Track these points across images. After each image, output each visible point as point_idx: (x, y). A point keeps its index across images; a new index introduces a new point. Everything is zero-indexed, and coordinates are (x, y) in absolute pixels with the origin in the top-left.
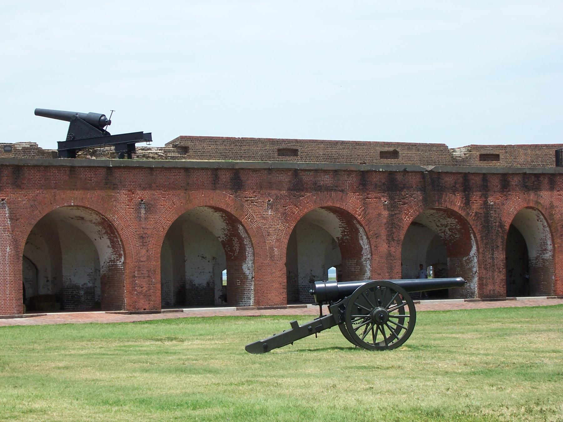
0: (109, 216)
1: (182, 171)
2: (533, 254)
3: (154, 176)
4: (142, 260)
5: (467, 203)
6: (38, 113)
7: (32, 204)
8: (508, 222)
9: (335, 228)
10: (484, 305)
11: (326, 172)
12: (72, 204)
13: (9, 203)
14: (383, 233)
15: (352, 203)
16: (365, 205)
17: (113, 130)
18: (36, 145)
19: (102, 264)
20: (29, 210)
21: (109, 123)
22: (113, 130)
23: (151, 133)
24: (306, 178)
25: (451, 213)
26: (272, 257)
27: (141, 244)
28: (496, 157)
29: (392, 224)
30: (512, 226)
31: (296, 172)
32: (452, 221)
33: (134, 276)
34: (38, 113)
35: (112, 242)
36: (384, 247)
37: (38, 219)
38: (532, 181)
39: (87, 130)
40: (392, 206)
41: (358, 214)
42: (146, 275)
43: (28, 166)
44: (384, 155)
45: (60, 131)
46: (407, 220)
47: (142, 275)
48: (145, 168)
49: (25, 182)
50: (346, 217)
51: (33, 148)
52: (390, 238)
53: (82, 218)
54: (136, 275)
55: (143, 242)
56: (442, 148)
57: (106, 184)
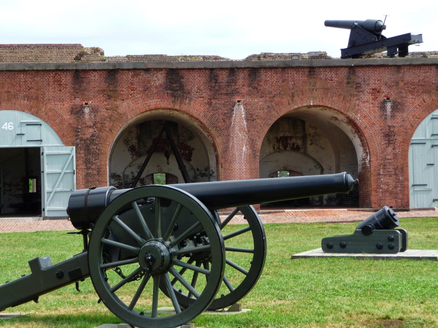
0: (352, 115)
1: (434, 68)
3: (402, 74)
4: (388, 157)
6: (328, 24)
7: (269, 104)
12: (312, 104)
13: (245, 105)
17: (387, 34)
18: (325, 53)
19: (359, 163)
20: (265, 110)
21: (383, 28)
22: (387, 34)
23: (421, 35)
27: (387, 142)
33: (379, 174)
34: (328, 24)
35: (362, 141)
37: (275, 119)
39: (366, 36)
42: (393, 173)
43: (265, 68)
45: (341, 39)
47: (388, 173)
48: (391, 66)
49: (262, 84)
51: (322, 56)
53: (336, 119)
54: (381, 173)
55: (389, 140)
57: (348, 83)
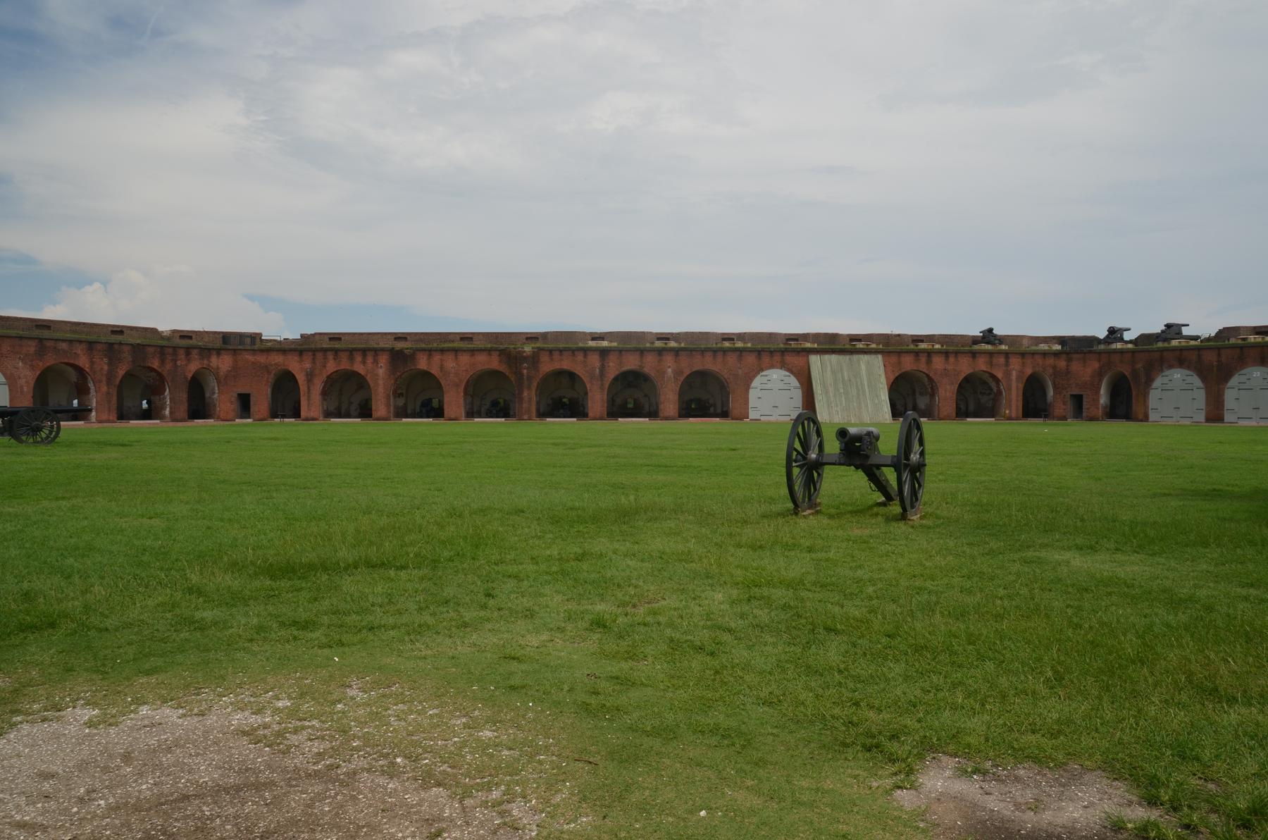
2: (207, 395)
5: (163, 362)
8: (190, 376)
9: (73, 376)
10: (171, 424)
11: (63, 341)
14: (104, 379)
15: (83, 362)
16: (92, 363)
24: (48, 344)
25: (152, 370)
26: (22, 392)
28: (190, 338)
29: (110, 377)
30: (194, 377)
31: (41, 340)
32: (153, 374)
36: (104, 389)
38: (206, 351)
40: (110, 364)
41: (87, 367)
44: (113, 332)
46: (121, 373)
50: (79, 370)
52: (109, 383)
56: (154, 331)
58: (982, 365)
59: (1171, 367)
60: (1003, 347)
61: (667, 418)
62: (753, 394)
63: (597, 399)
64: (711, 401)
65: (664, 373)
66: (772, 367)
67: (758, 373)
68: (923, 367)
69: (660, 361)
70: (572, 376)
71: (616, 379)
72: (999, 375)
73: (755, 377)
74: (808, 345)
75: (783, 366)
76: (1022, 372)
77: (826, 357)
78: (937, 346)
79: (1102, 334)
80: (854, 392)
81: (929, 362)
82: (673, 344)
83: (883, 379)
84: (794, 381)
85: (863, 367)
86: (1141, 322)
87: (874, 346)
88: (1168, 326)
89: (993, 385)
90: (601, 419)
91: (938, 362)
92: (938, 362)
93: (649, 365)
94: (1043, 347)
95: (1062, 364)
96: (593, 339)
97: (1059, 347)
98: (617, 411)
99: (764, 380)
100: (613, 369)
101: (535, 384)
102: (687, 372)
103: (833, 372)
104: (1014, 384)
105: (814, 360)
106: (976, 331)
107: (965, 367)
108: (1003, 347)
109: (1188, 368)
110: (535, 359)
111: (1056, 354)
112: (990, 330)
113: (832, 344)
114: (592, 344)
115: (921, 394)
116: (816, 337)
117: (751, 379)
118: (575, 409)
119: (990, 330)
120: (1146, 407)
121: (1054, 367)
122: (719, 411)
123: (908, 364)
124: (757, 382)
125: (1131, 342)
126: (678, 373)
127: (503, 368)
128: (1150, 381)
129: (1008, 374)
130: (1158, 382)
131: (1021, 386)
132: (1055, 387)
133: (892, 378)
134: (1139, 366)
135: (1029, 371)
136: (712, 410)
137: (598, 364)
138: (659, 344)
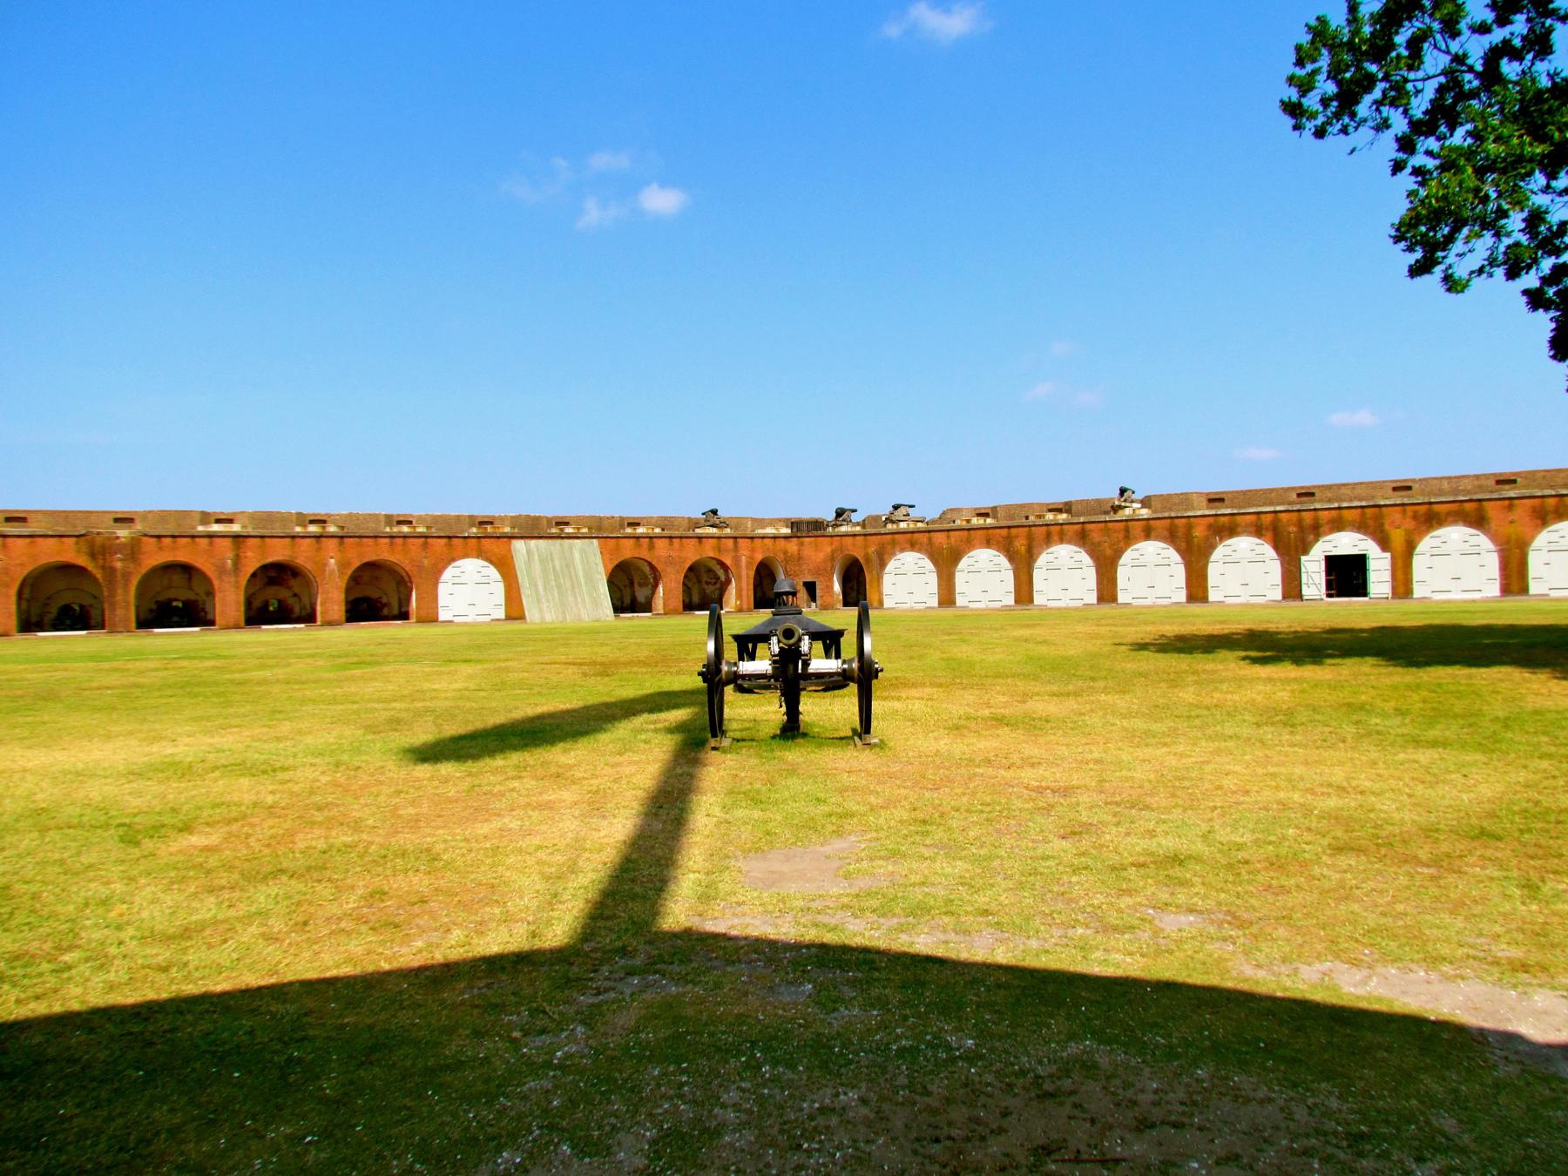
58: (708, 551)
59: (903, 550)
60: (728, 531)
61: (329, 624)
62: (443, 590)
63: (229, 599)
64: (384, 600)
65: (325, 565)
66: (466, 556)
67: (449, 563)
68: (645, 554)
69: (319, 550)
70: (187, 570)
71: (254, 575)
72: (728, 562)
73: (445, 568)
74: (507, 530)
75: (480, 554)
76: (752, 558)
77: (533, 542)
78: (657, 530)
79: (831, 516)
80: (568, 584)
81: (651, 547)
82: (332, 529)
83: (601, 569)
84: (493, 573)
85: (577, 555)
86: (870, 504)
87: (585, 530)
88: (896, 507)
89: (721, 573)
90: (237, 627)
91: (661, 544)
92: (661, 544)
93: (302, 555)
94: (770, 531)
95: (792, 547)
96: (218, 521)
97: (786, 531)
98: (257, 616)
99: (457, 572)
100: (252, 562)
101: (135, 582)
102: (356, 564)
103: (542, 561)
104: (744, 573)
105: (519, 546)
106: (695, 510)
107: (691, 554)
108: (728, 531)
109: (919, 551)
110: (133, 550)
111: (786, 537)
112: (714, 512)
113: (533, 529)
114: (216, 528)
115: (641, 585)
116: (515, 521)
117: (440, 572)
118: (194, 614)
119: (714, 512)
120: (880, 593)
121: (785, 553)
122: (396, 612)
123: (628, 551)
124: (448, 574)
125: (858, 524)
126: (343, 565)
127: (82, 561)
128: (883, 565)
129: (737, 560)
130: (891, 566)
131: (752, 574)
132: (787, 574)
133: (611, 567)
134: (872, 549)
135: (759, 557)
136: (385, 612)
137: (230, 554)
138: (313, 529)
